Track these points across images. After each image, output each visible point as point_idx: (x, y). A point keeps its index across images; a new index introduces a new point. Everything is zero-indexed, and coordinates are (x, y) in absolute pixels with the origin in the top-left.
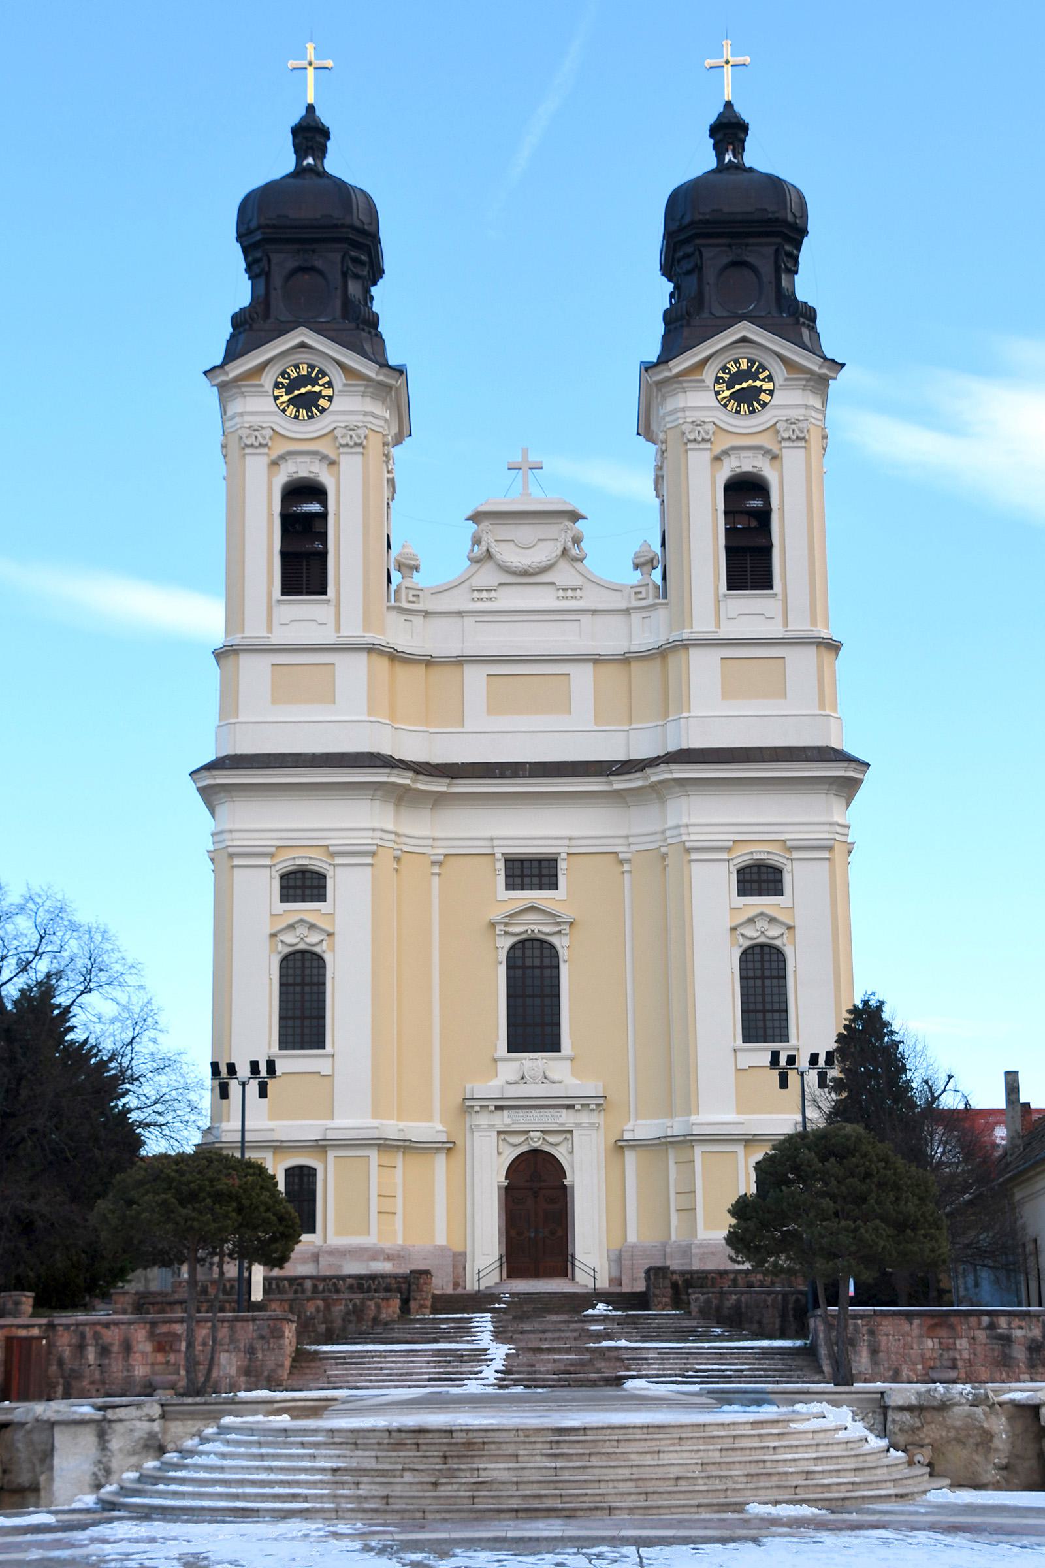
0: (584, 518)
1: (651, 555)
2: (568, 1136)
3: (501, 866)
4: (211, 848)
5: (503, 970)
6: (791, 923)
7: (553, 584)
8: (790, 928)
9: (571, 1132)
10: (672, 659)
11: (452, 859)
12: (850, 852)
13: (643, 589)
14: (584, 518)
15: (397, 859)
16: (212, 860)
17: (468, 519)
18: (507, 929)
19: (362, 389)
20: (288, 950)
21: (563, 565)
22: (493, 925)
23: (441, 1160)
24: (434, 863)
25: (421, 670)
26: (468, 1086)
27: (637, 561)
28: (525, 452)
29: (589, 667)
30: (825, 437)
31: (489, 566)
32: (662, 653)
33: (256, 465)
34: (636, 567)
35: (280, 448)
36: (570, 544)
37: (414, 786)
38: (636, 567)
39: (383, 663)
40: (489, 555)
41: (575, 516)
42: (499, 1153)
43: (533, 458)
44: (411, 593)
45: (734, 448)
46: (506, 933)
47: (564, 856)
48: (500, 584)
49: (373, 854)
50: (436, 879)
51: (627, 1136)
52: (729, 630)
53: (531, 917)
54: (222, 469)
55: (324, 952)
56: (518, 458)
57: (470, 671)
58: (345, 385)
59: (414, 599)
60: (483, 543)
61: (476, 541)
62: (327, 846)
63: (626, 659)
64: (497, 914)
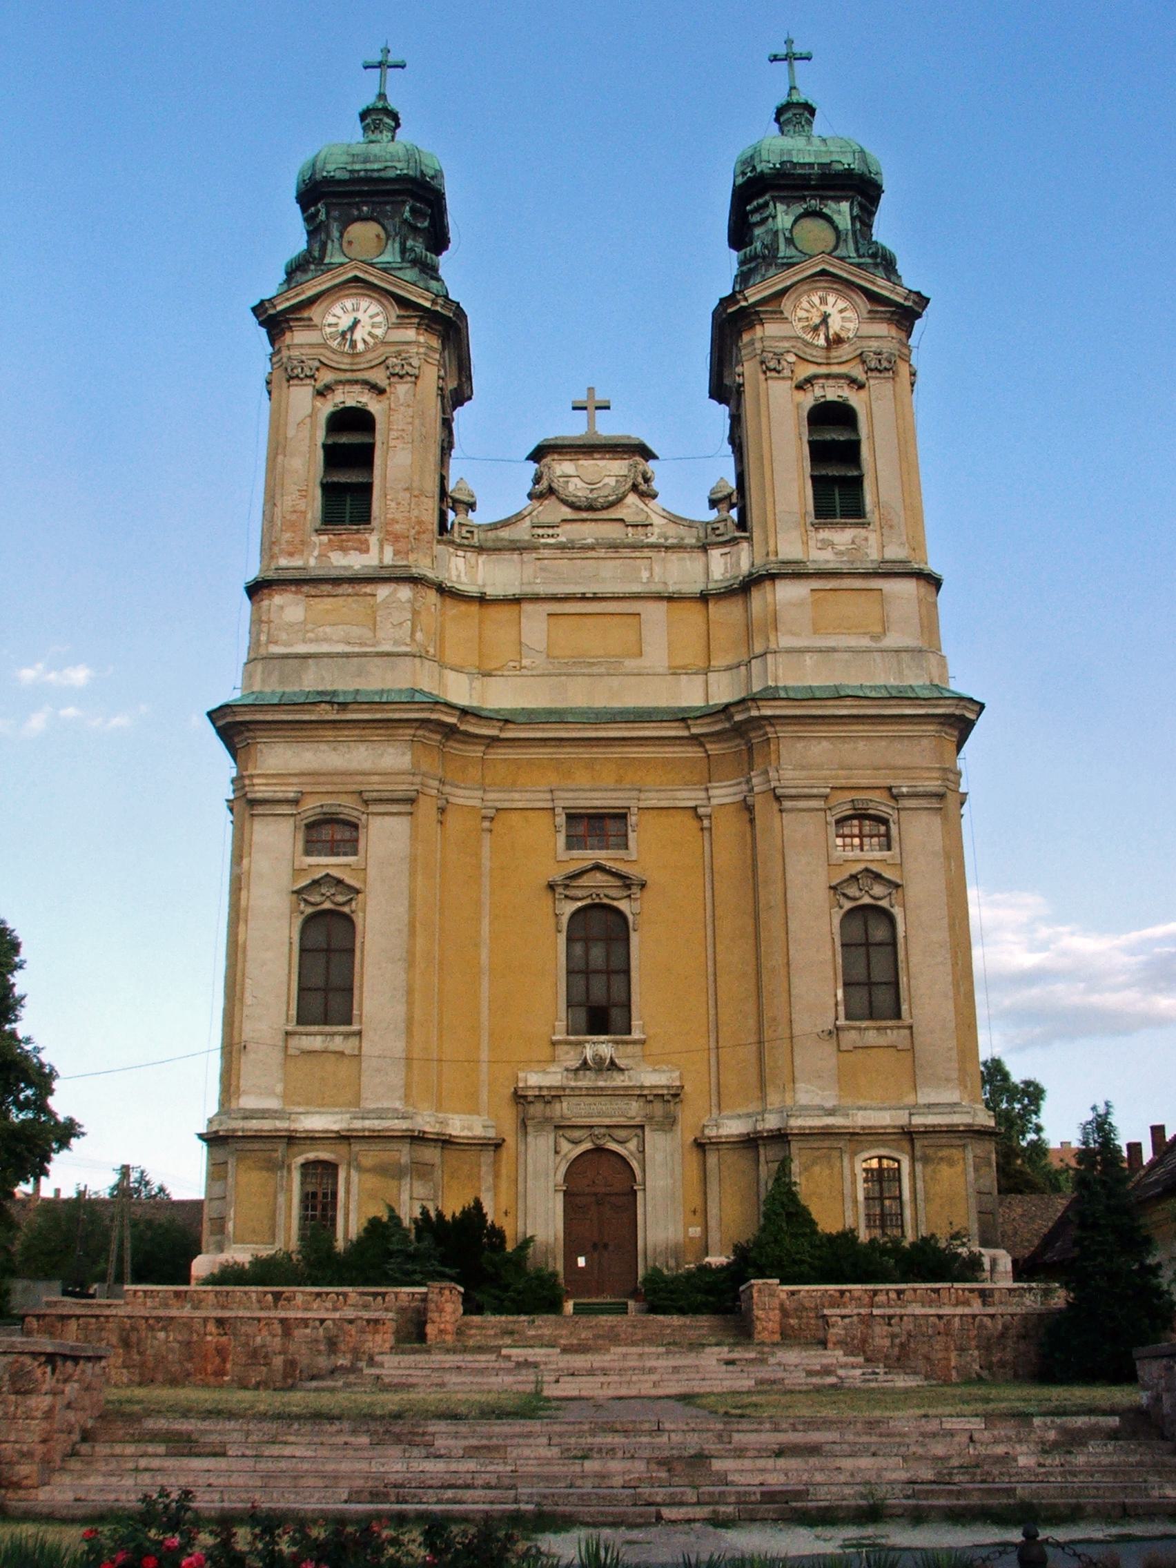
0: (654, 457)
1: (729, 491)
2: (639, 1131)
3: (561, 820)
4: (231, 797)
5: (562, 938)
6: (899, 881)
7: (622, 520)
8: (897, 886)
9: (642, 1127)
10: (756, 594)
11: (503, 815)
12: (962, 804)
13: (721, 525)
14: (654, 457)
15: (442, 810)
16: (231, 810)
17: (528, 458)
18: (567, 893)
19: (416, 320)
20: (310, 910)
21: (632, 499)
22: (551, 887)
23: (487, 1157)
24: (484, 818)
25: (474, 608)
26: (521, 1075)
27: (714, 497)
28: (591, 390)
29: (664, 605)
30: (913, 374)
31: (551, 502)
32: (746, 587)
33: (301, 397)
34: (713, 503)
35: (326, 377)
36: (640, 480)
37: (463, 728)
38: (713, 503)
39: (432, 596)
40: (551, 491)
41: (646, 453)
42: (557, 1152)
43: (600, 397)
44: (464, 529)
45: (816, 377)
46: (566, 897)
47: (634, 810)
48: (564, 521)
49: (412, 801)
50: (487, 836)
51: (711, 1132)
52: (822, 557)
53: (599, 877)
54: (266, 405)
55: (353, 912)
56: (582, 397)
57: (527, 607)
58: (398, 317)
59: (468, 535)
60: (545, 478)
61: (537, 479)
62: (361, 793)
63: (704, 598)
64: (557, 875)
